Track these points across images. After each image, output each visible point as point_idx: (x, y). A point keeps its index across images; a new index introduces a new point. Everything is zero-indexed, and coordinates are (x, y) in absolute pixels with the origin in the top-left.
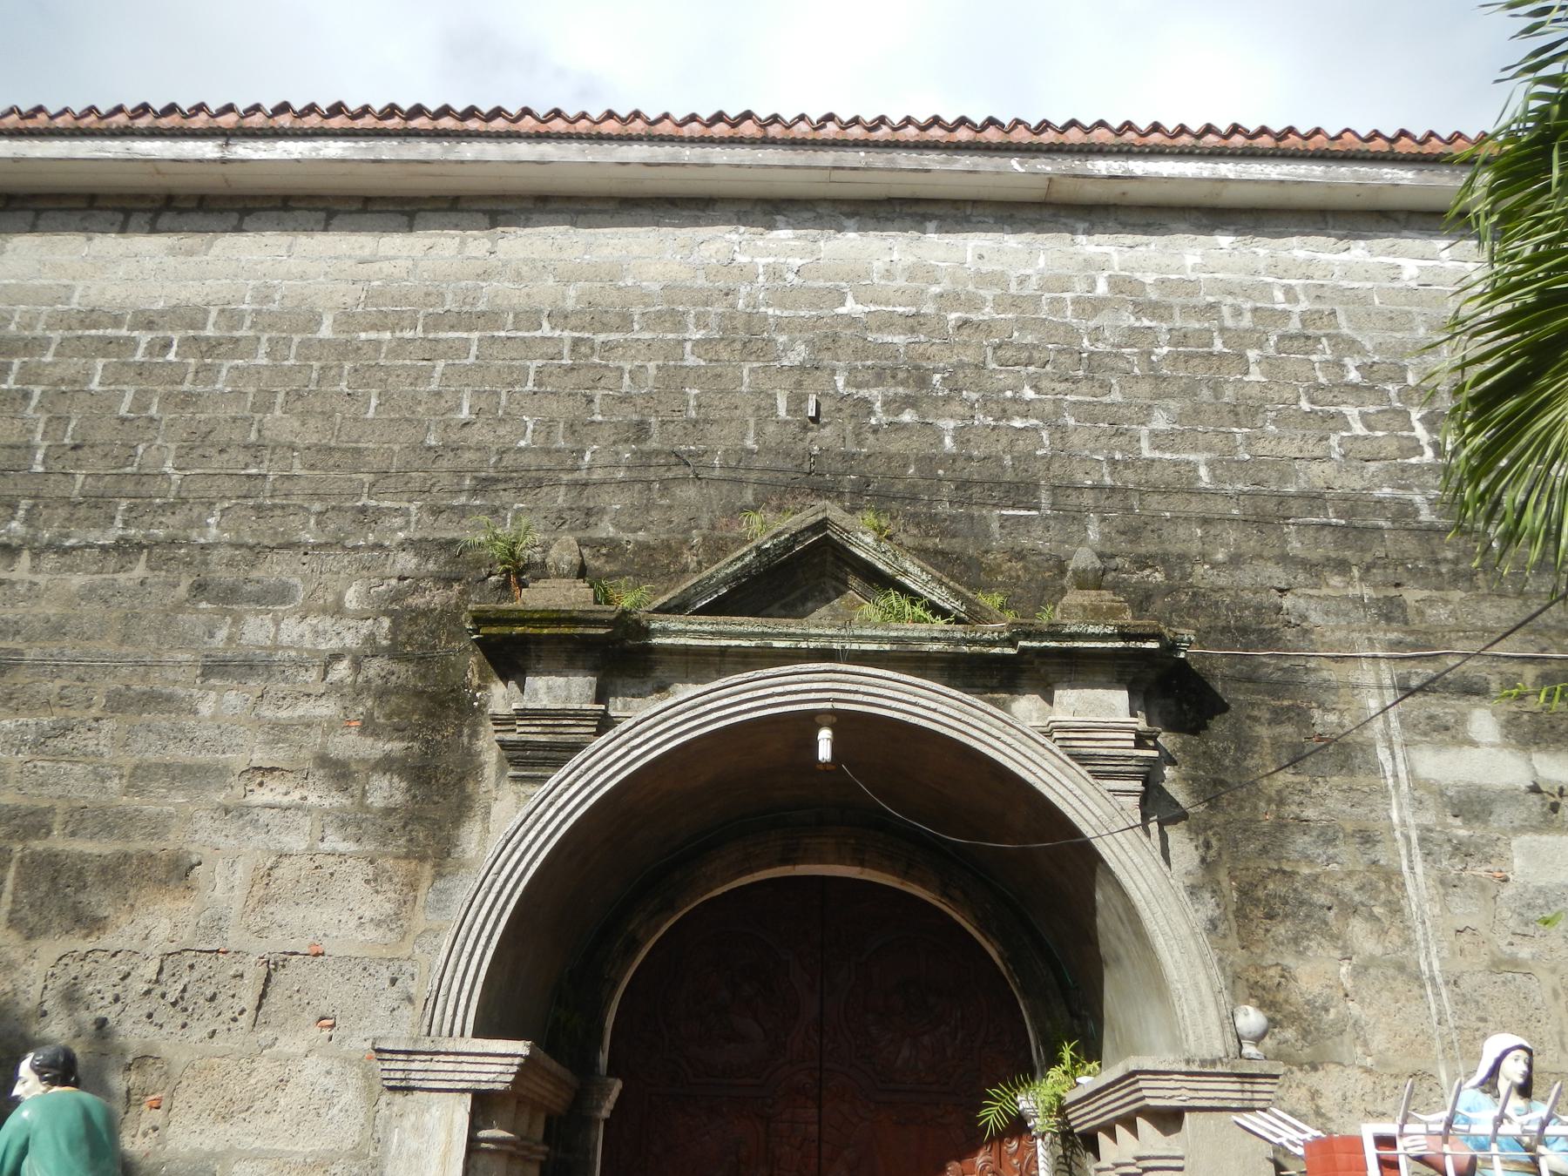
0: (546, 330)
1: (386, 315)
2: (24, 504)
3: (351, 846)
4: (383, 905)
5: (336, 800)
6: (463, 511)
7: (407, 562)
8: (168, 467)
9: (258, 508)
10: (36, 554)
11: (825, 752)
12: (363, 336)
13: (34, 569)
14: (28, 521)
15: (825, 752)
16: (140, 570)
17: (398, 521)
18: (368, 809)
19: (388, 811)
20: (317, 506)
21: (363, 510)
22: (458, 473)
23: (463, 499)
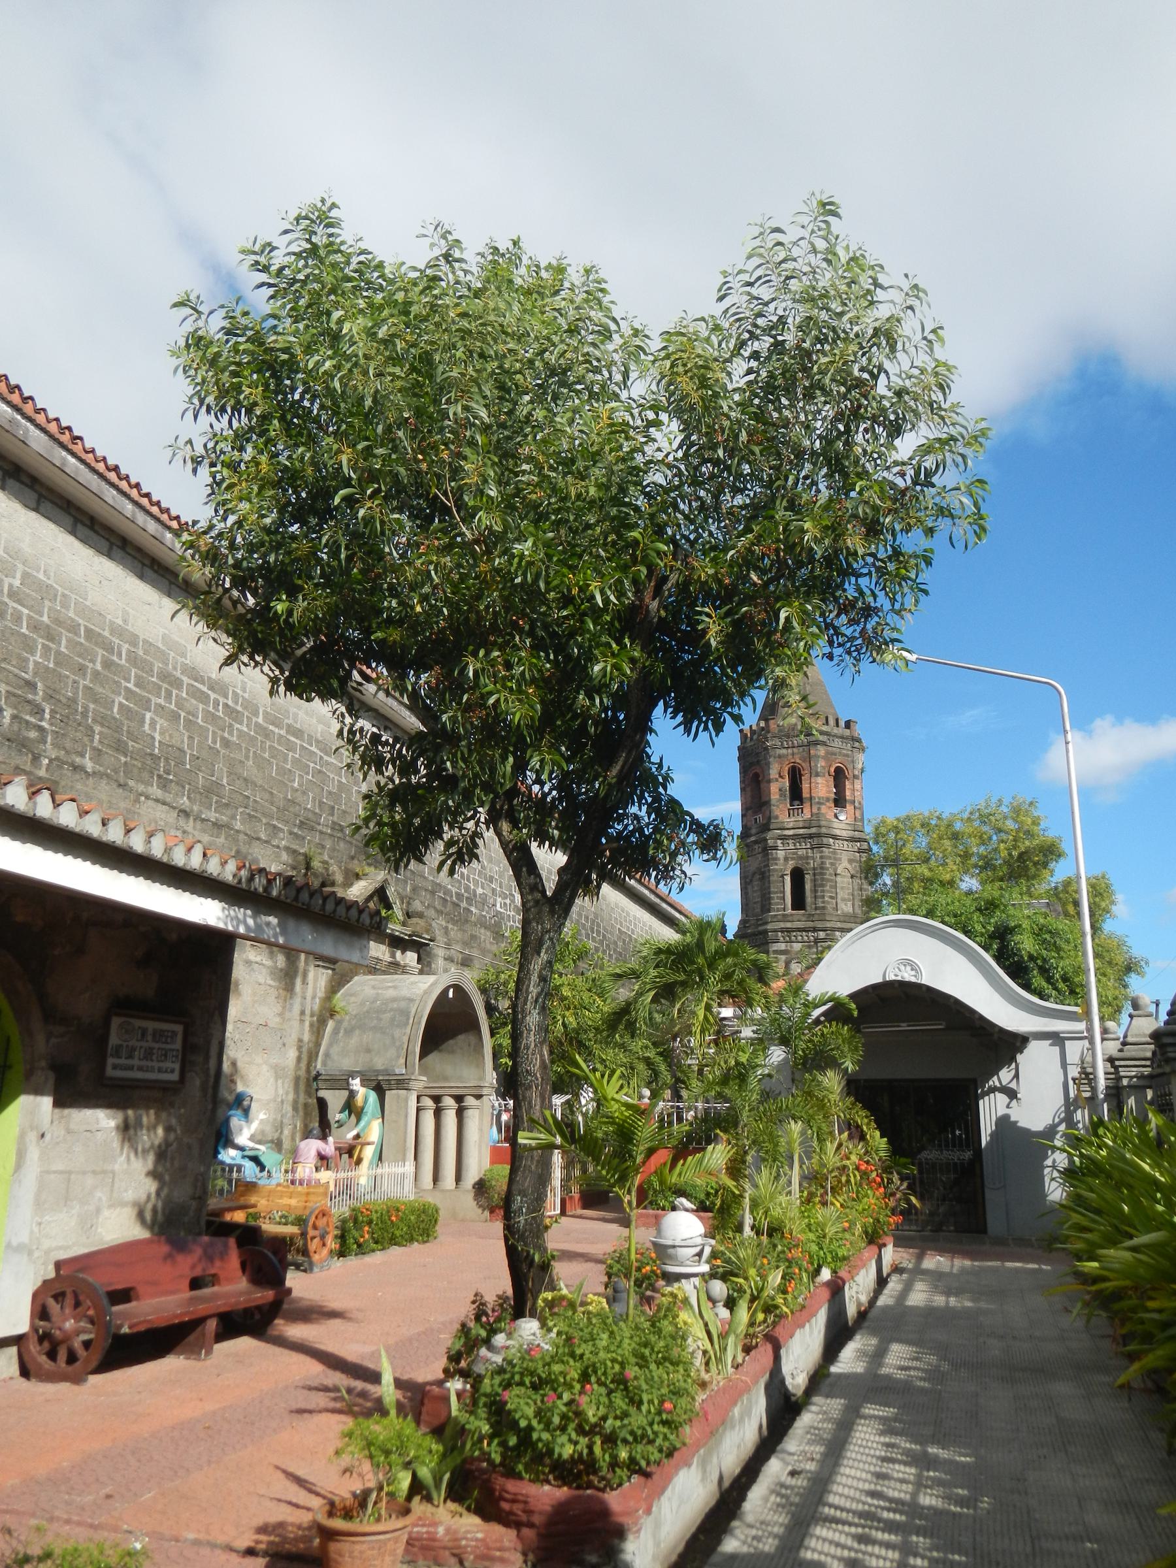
0: (313, 749)
1: (276, 717)
2: (187, 787)
3: (272, 983)
4: (278, 1008)
5: (269, 963)
6: (296, 834)
7: (285, 856)
8: (225, 781)
9: (249, 814)
10: (195, 820)
11: (451, 995)
12: (271, 727)
13: (194, 828)
14: (189, 798)
15: (451, 995)
16: (222, 840)
17: (281, 835)
18: (276, 967)
19: (281, 970)
20: (264, 821)
21: (275, 827)
22: (297, 815)
23: (296, 830)
